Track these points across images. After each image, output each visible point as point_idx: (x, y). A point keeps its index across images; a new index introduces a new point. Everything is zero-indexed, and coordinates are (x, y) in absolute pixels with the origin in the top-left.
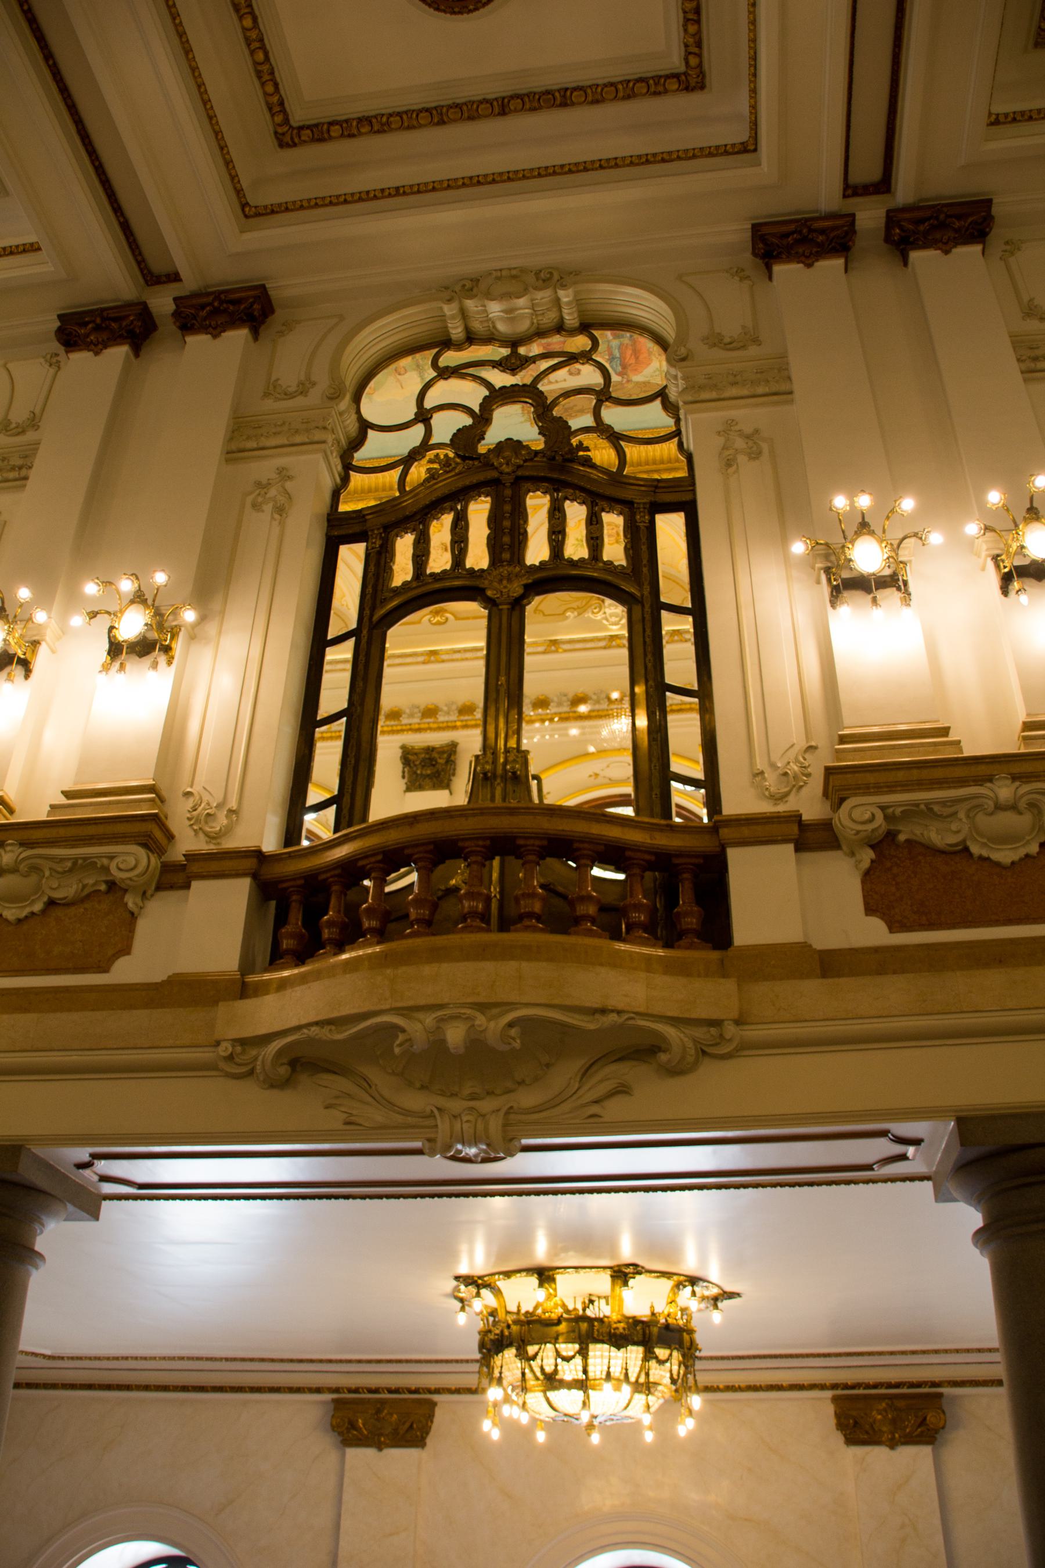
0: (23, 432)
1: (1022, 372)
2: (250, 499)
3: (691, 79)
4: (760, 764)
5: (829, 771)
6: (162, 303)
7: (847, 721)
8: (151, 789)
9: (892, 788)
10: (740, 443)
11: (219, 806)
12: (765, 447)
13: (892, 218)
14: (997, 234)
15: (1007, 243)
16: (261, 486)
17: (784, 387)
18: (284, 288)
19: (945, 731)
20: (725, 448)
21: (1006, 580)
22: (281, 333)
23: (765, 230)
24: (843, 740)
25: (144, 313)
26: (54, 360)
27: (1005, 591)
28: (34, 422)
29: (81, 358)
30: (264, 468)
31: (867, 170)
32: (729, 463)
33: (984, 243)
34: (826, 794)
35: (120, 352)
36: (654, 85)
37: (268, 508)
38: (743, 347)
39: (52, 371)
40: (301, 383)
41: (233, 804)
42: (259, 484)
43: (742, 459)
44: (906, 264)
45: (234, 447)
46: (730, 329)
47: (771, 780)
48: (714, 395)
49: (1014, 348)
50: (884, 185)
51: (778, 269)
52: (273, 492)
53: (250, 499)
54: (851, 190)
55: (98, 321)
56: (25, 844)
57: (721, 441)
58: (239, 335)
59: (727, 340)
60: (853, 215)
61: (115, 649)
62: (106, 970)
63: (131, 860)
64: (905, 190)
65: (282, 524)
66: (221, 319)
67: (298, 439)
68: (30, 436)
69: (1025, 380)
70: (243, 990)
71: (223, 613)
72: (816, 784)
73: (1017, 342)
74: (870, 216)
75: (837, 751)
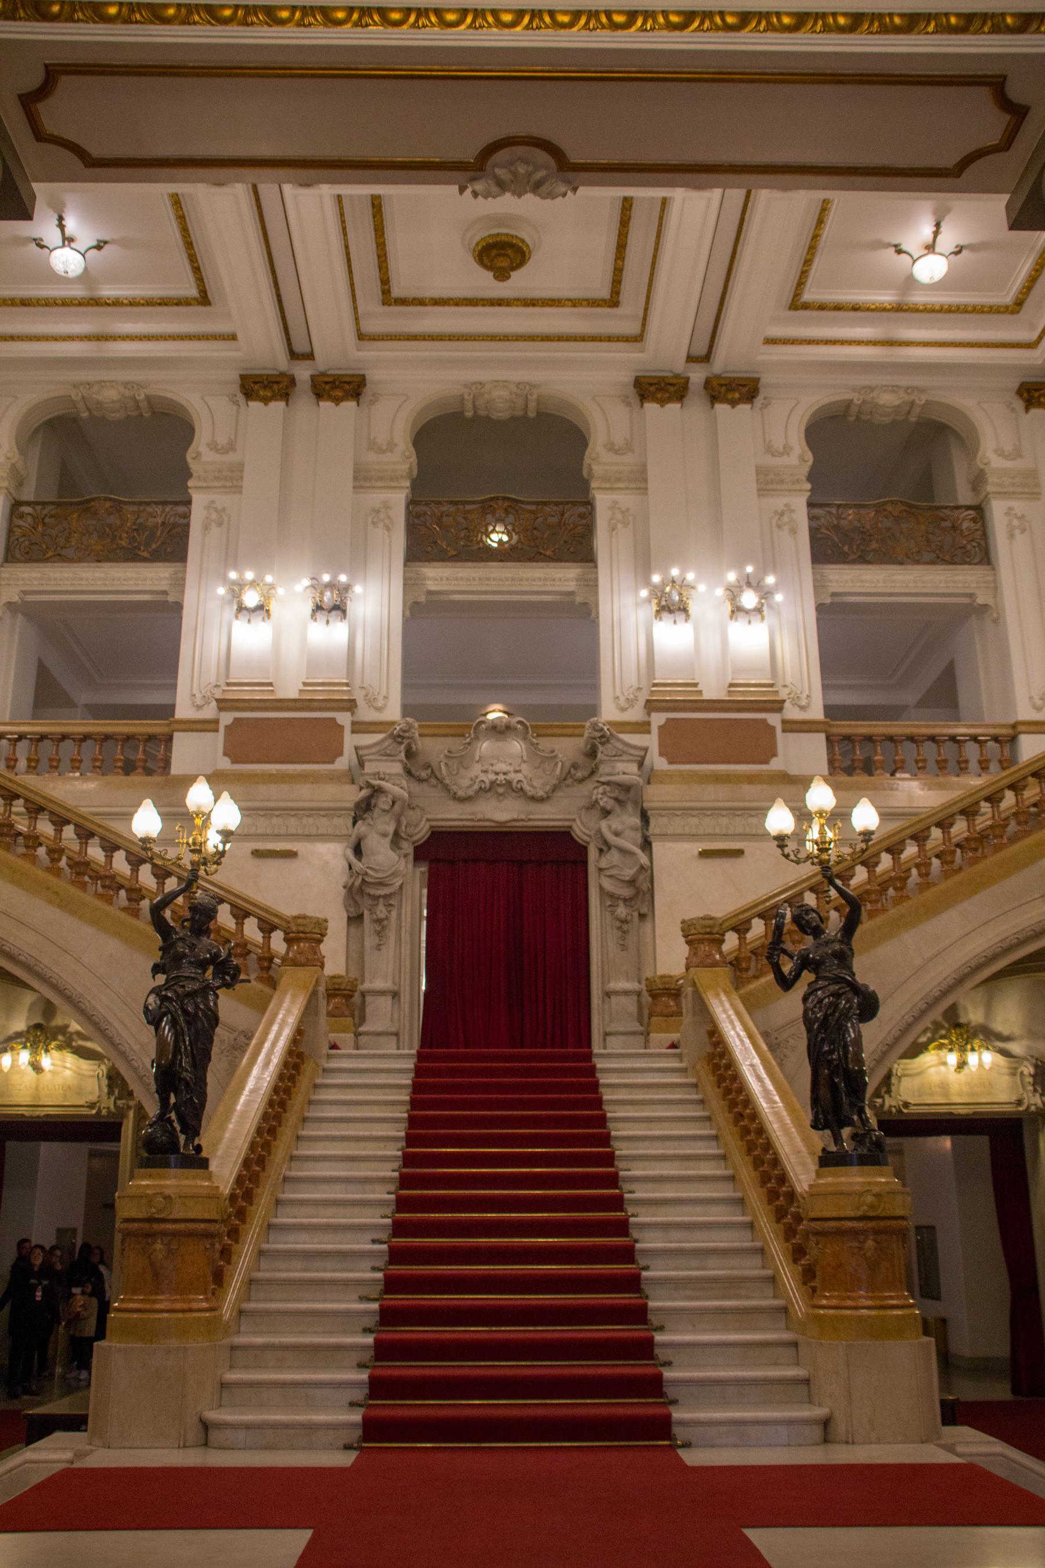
0: (227, 452)
1: (758, 490)
2: (370, 519)
3: (613, 302)
4: (618, 693)
5: (648, 701)
6: (303, 373)
7: (657, 676)
8: (347, 685)
10: (619, 516)
12: (631, 519)
13: (708, 384)
14: (759, 401)
15: (765, 399)
17: (643, 485)
18: (373, 375)
19: (695, 685)
20: (612, 518)
21: (733, 612)
22: (372, 402)
23: (643, 380)
24: (655, 685)
25: (292, 381)
26: (235, 399)
27: (731, 618)
28: (231, 447)
29: (255, 405)
31: (701, 349)
33: (752, 403)
34: (645, 707)
35: (278, 406)
36: (593, 303)
37: (381, 525)
38: (624, 454)
39: (235, 407)
40: (389, 443)
41: (384, 693)
42: (374, 510)
43: (620, 526)
44: (712, 407)
45: (357, 484)
46: (619, 441)
47: (622, 699)
48: (608, 486)
49: (757, 474)
50: (706, 358)
51: (647, 405)
52: (382, 515)
54: (690, 359)
55: (266, 382)
57: (610, 513)
58: (349, 405)
59: (616, 447)
60: (688, 379)
61: (318, 608)
64: (719, 365)
66: (339, 393)
67: (393, 484)
68: (232, 458)
69: (759, 495)
72: (641, 703)
73: (759, 470)
74: (697, 376)
75: (652, 691)
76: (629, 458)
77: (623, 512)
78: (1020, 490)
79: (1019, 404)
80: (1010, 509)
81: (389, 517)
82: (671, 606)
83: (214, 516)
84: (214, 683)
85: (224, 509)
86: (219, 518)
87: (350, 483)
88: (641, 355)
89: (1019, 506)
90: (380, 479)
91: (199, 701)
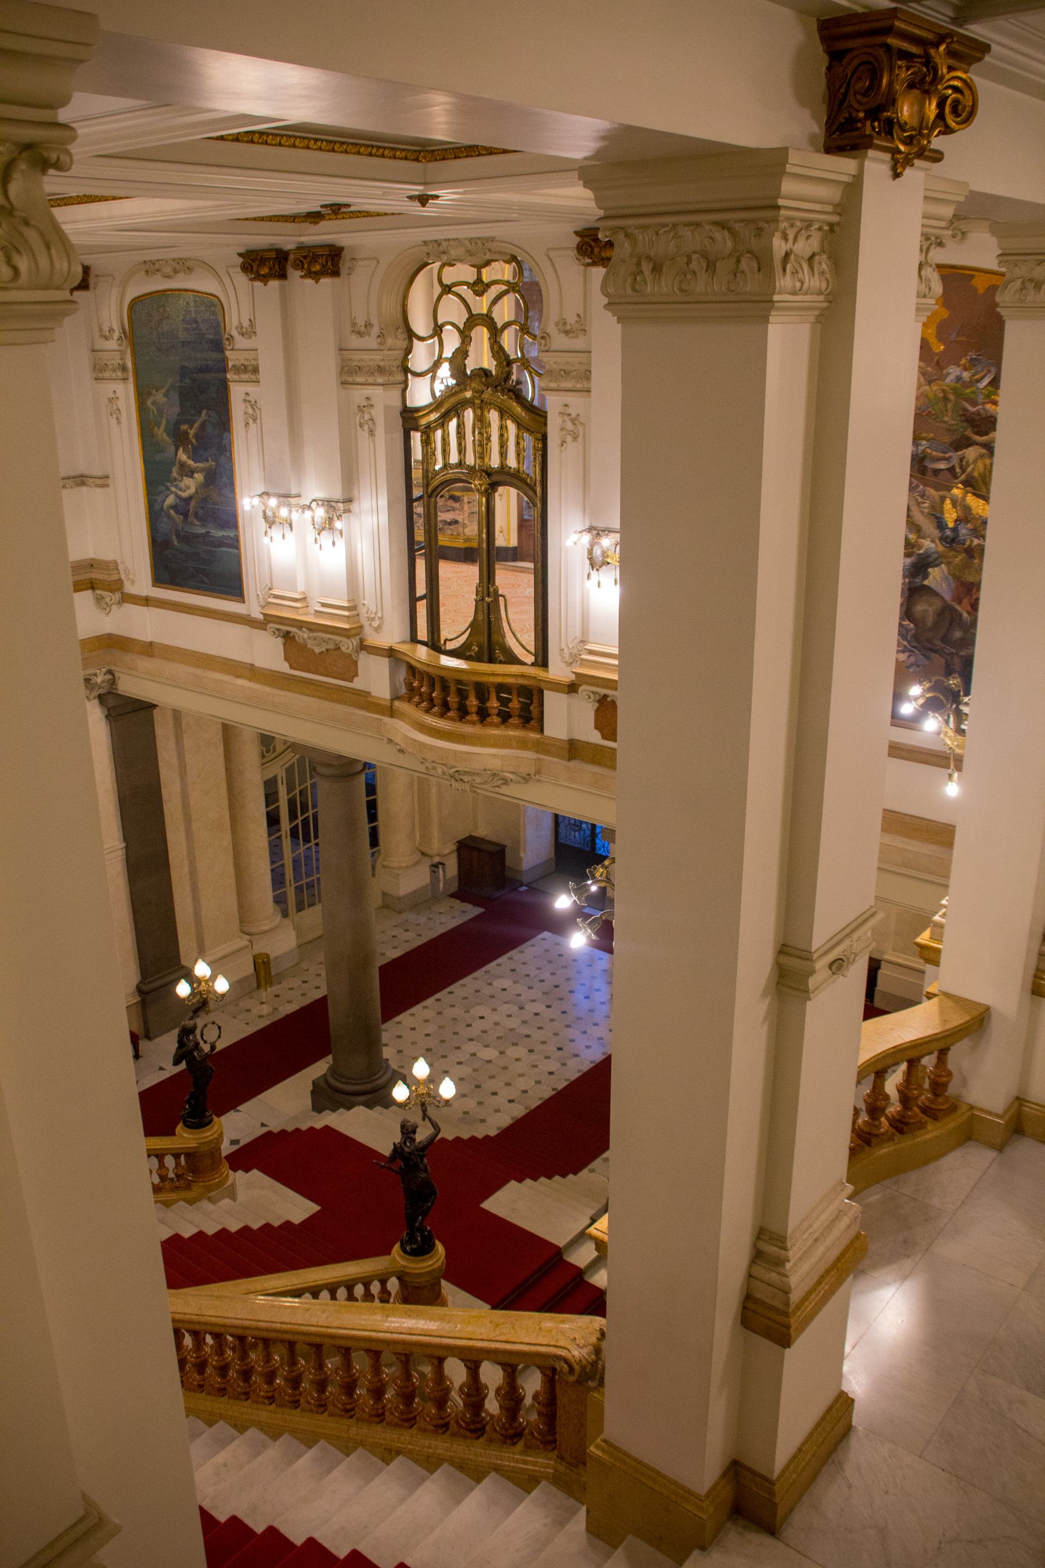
4: (563, 646)
9: (598, 686)
11: (376, 613)
16: (361, 409)
30: (358, 394)
41: (379, 615)
56: (310, 630)
63: (348, 646)
65: (373, 441)
70: (392, 712)
71: (359, 499)
77: (573, 421)
81: (372, 420)
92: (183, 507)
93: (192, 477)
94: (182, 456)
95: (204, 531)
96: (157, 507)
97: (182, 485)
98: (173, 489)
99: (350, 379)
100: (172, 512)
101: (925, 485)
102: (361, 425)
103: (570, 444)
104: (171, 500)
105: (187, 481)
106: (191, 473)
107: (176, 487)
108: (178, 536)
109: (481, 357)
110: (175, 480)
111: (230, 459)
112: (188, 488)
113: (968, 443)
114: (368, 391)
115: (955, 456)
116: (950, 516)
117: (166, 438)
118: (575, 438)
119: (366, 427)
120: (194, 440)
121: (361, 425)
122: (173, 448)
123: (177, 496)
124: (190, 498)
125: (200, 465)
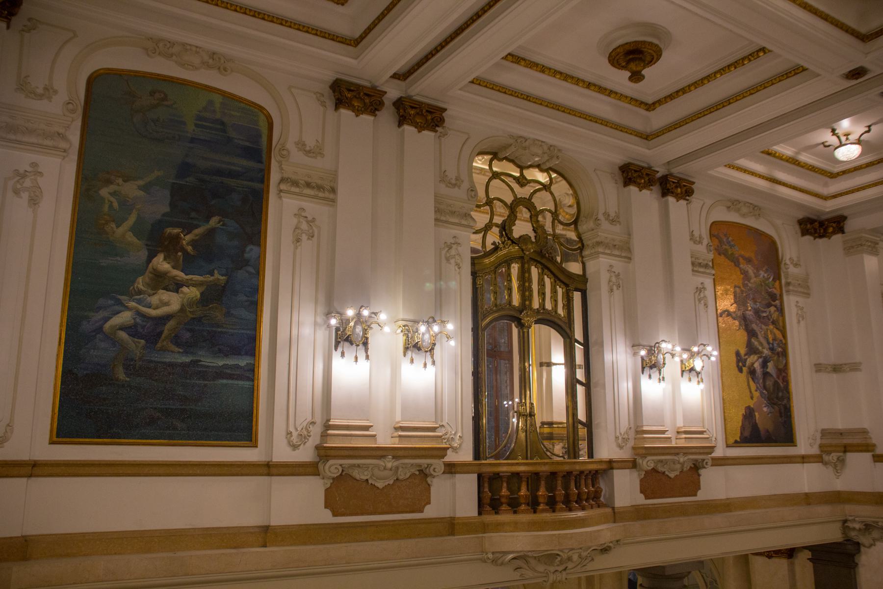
2: (444, 252)
4: (618, 434)
11: (455, 434)
17: (629, 255)
32: (612, 290)
39: (322, 108)
41: (459, 434)
53: (444, 252)
56: (395, 457)
62: (422, 512)
76: (617, 228)
78: (802, 290)
79: (797, 228)
80: (797, 302)
81: (459, 255)
82: (651, 365)
83: (304, 226)
84: (309, 419)
85: (314, 220)
86: (305, 230)
87: (432, 215)
88: (647, 151)
89: (801, 300)
90: (453, 213)
91: (295, 438)
92: (150, 330)
93: (177, 291)
94: (161, 263)
95: (187, 359)
96: (86, 327)
97: (154, 300)
98: (133, 304)
99: (443, 218)
100: (123, 335)
101: (762, 323)
102: (448, 259)
103: (617, 293)
104: (125, 317)
105: (164, 295)
106: (177, 286)
107: (139, 302)
108: (127, 368)
109: (522, 228)
110: (140, 292)
111: (258, 272)
112: (167, 304)
113: (771, 305)
114: (455, 231)
115: (768, 310)
116: (770, 337)
117: (131, 237)
118: (619, 287)
119: (452, 261)
120: (189, 249)
121: (448, 259)
122: (144, 254)
123: (139, 313)
124: (168, 317)
125: (197, 278)
